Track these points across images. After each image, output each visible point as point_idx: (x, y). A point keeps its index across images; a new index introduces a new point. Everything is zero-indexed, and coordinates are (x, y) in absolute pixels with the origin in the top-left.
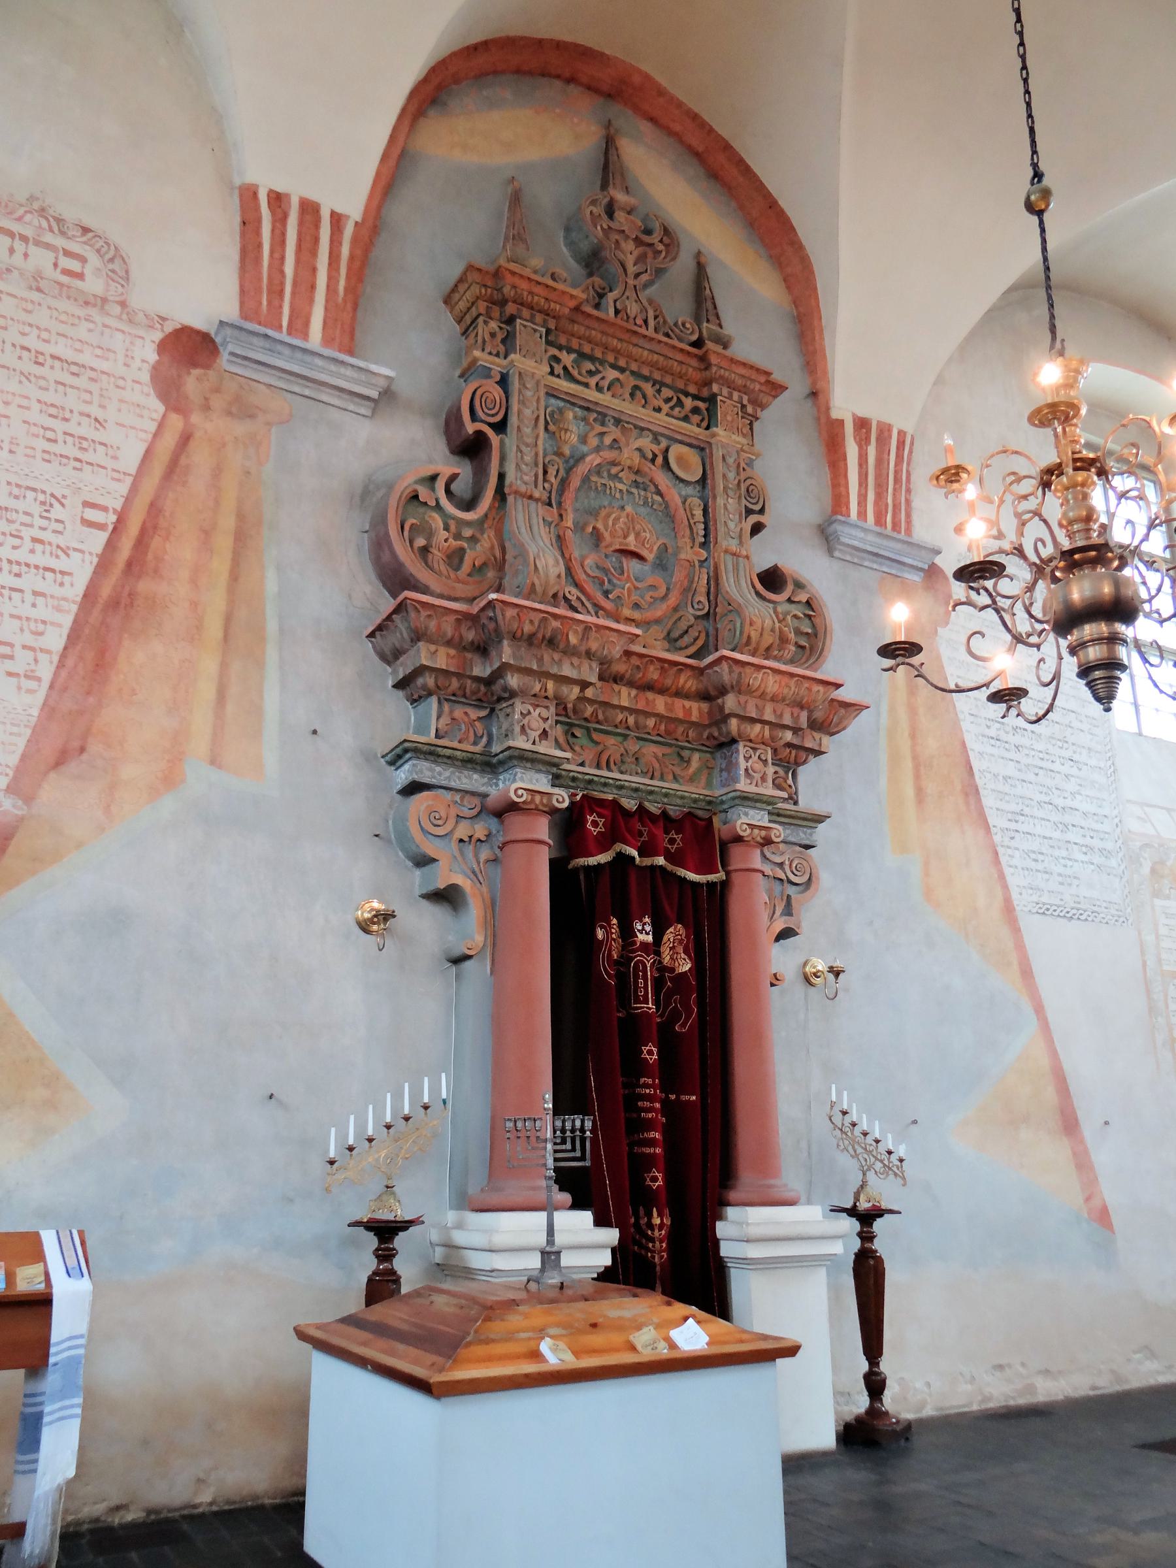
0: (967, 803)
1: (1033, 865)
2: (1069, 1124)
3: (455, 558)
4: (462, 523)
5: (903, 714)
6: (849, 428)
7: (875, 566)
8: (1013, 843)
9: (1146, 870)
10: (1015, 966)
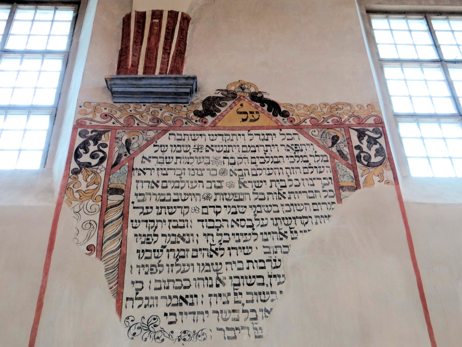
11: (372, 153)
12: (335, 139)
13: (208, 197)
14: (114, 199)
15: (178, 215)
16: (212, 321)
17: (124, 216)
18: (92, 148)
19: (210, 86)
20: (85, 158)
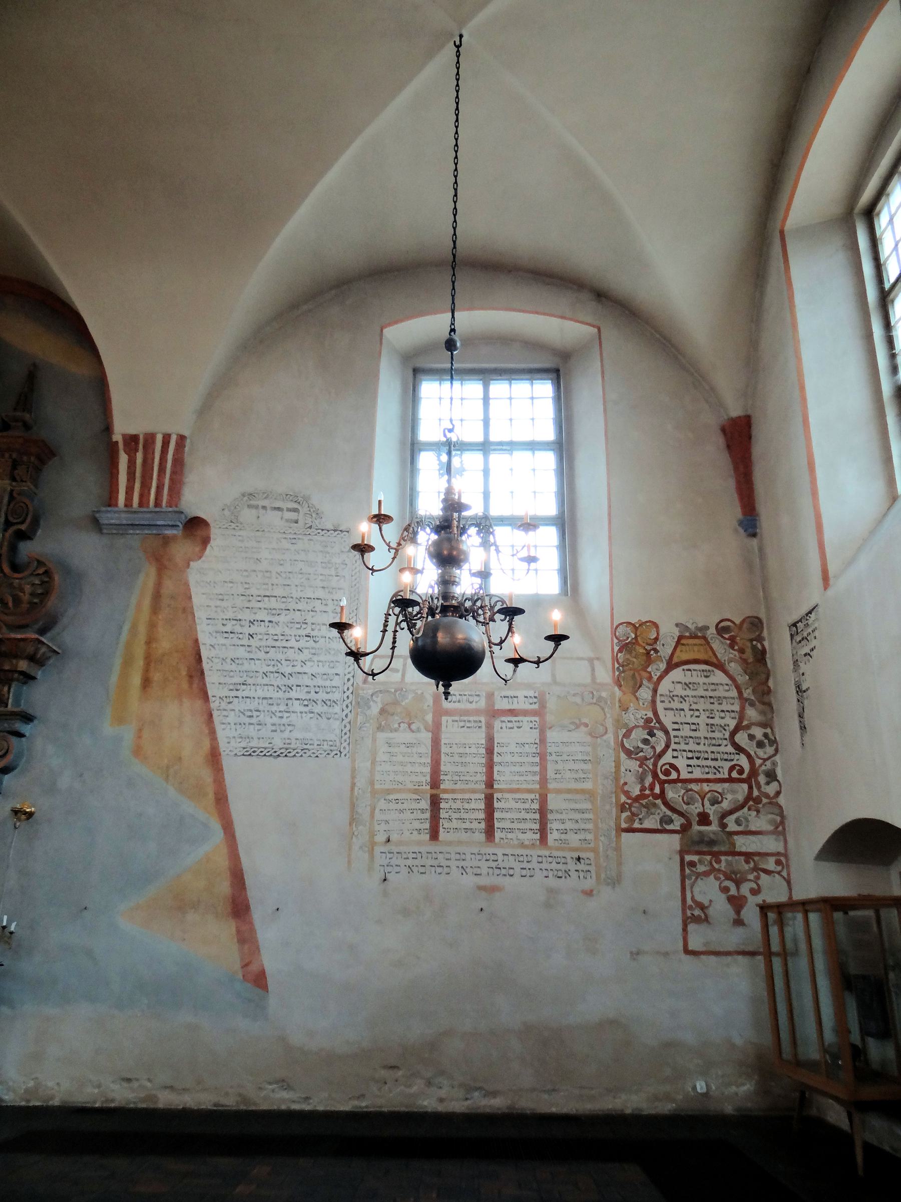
0: (191, 683)
1: (247, 720)
2: (239, 908)
5: (142, 629)
6: (121, 445)
7: (138, 532)
8: (231, 706)
9: (375, 709)
10: (211, 796)
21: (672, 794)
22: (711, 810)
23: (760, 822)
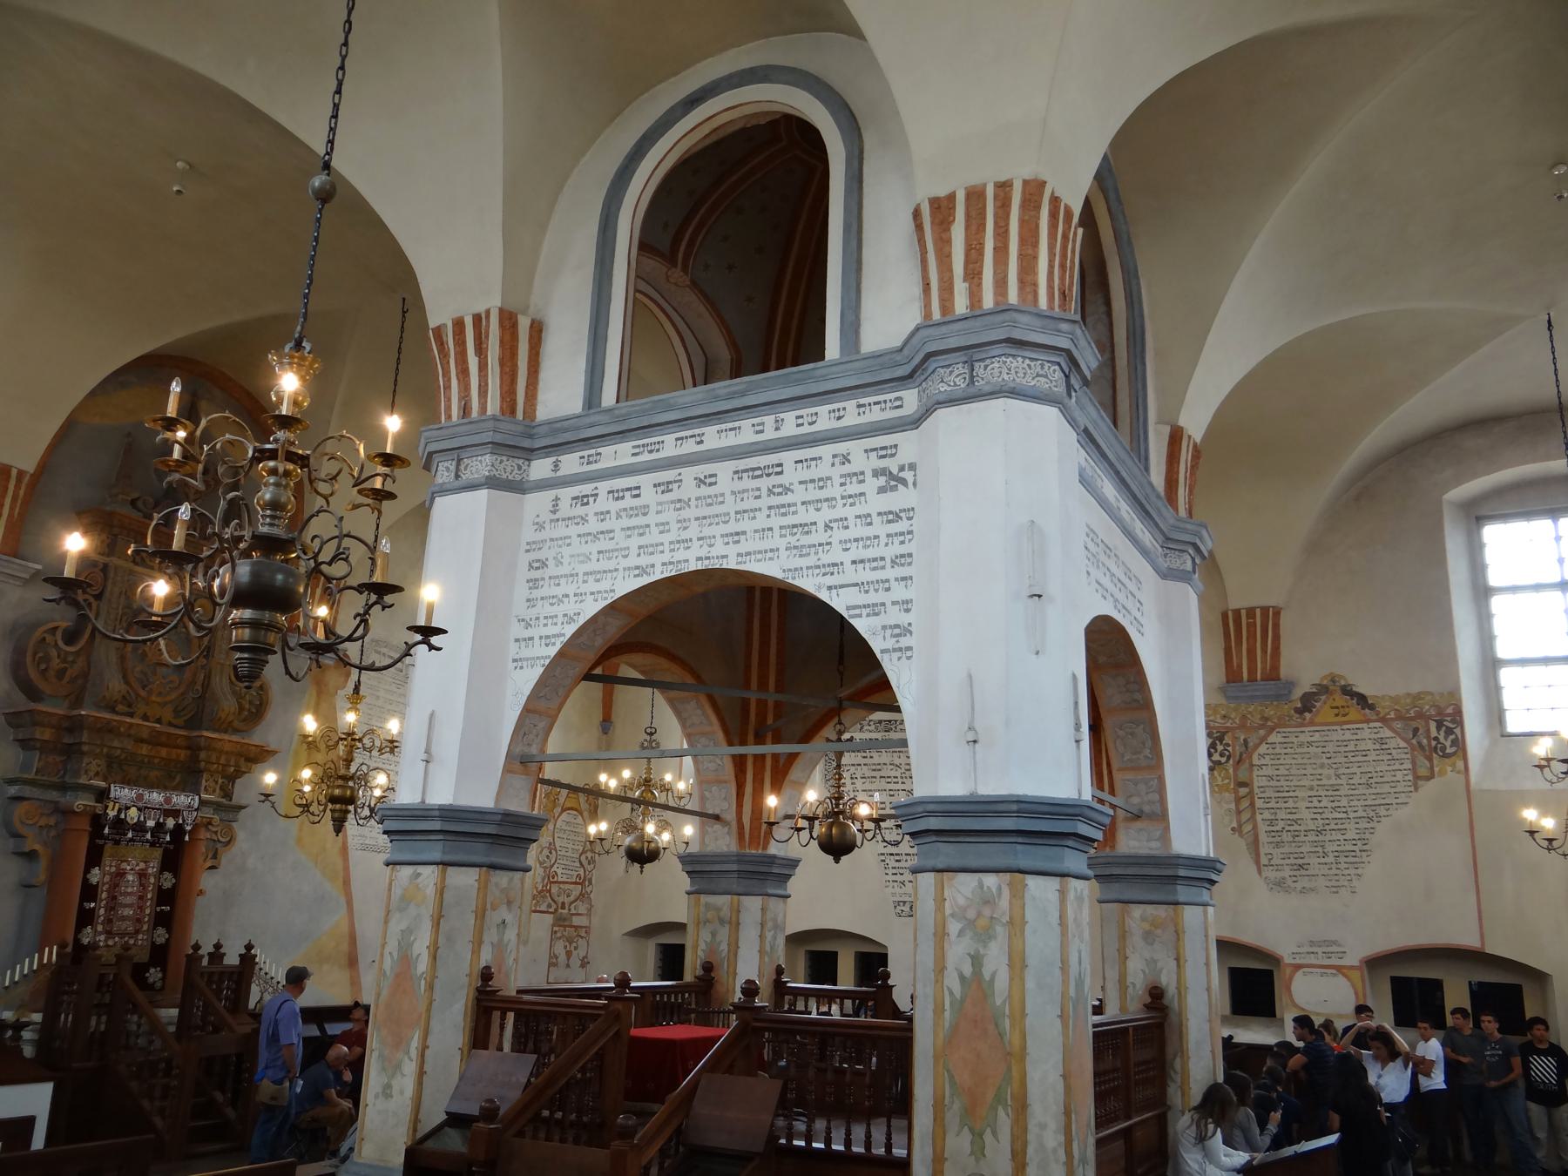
2: (352, 962)
3: (61, 674)
4: (67, 653)
11: (1448, 744)
12: (1416, 731)
13: (1311, 789)
14: (1243, 791)
15: (1290, 804)
16: (1322, 882)
17: (1252, 804)
18: (1220, 748)
19: (1305, 686)
20: (1216, 757)
21: (555, 889)
22: (567, 901)
23: (582, 909)
